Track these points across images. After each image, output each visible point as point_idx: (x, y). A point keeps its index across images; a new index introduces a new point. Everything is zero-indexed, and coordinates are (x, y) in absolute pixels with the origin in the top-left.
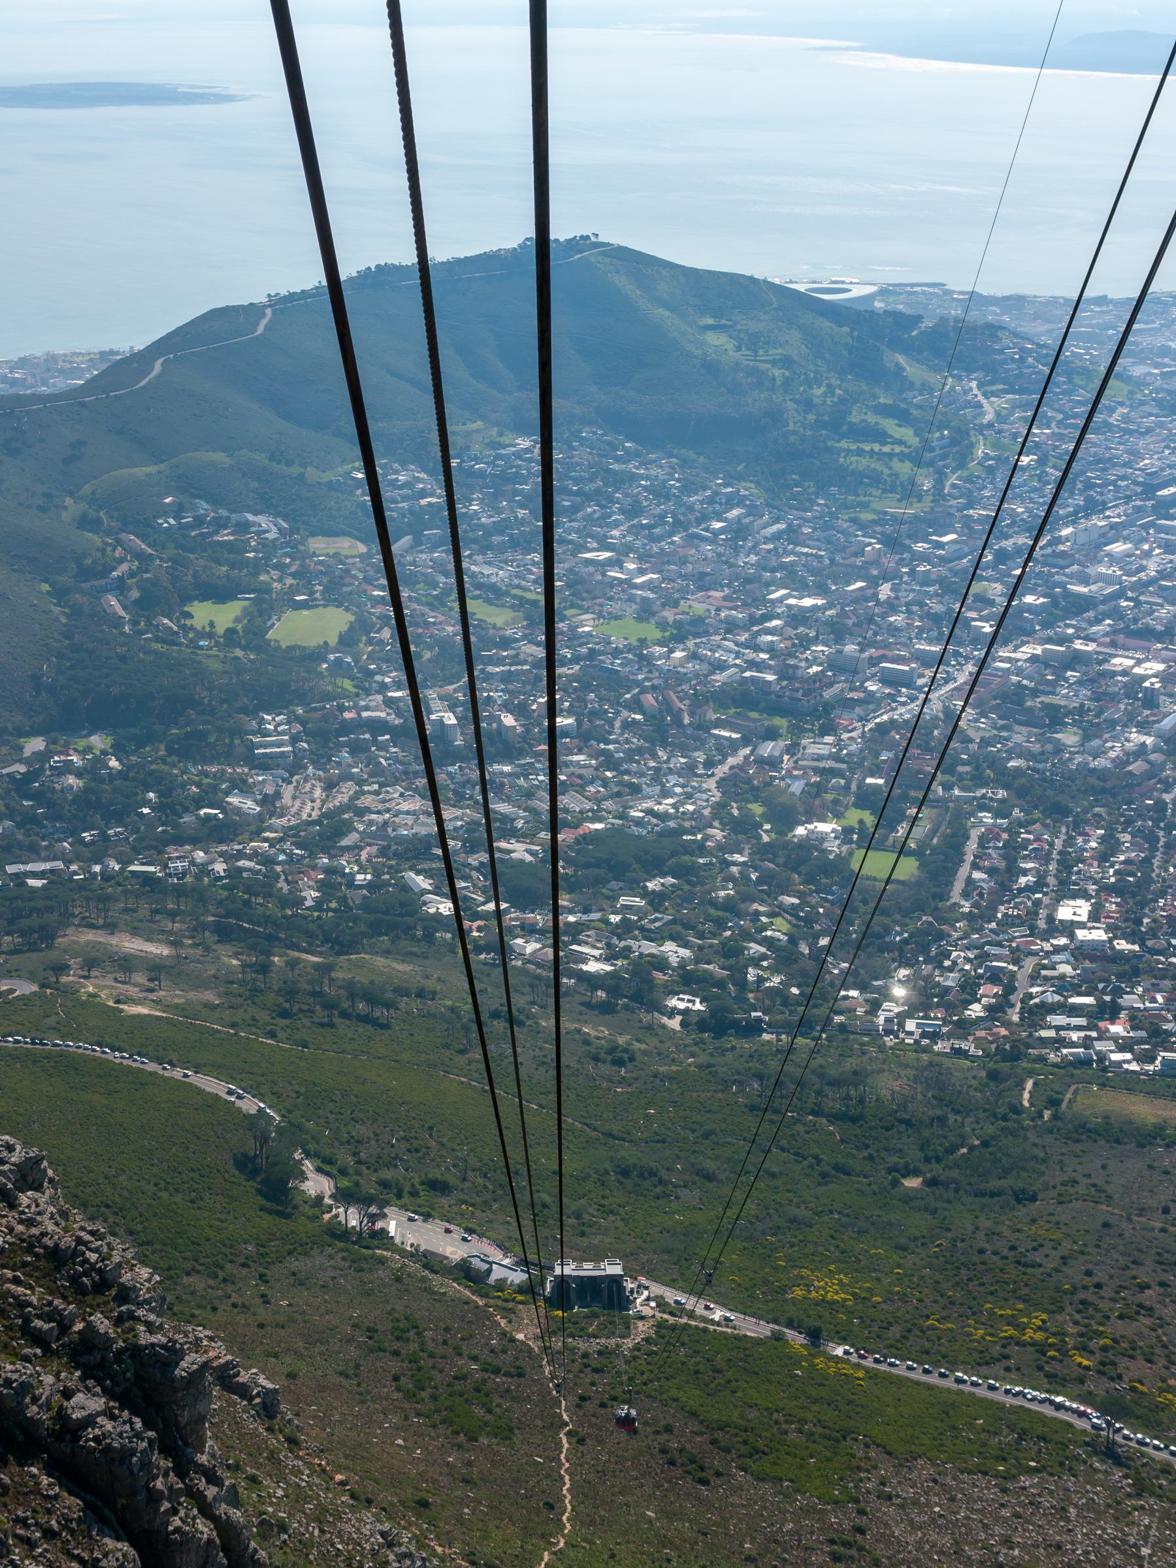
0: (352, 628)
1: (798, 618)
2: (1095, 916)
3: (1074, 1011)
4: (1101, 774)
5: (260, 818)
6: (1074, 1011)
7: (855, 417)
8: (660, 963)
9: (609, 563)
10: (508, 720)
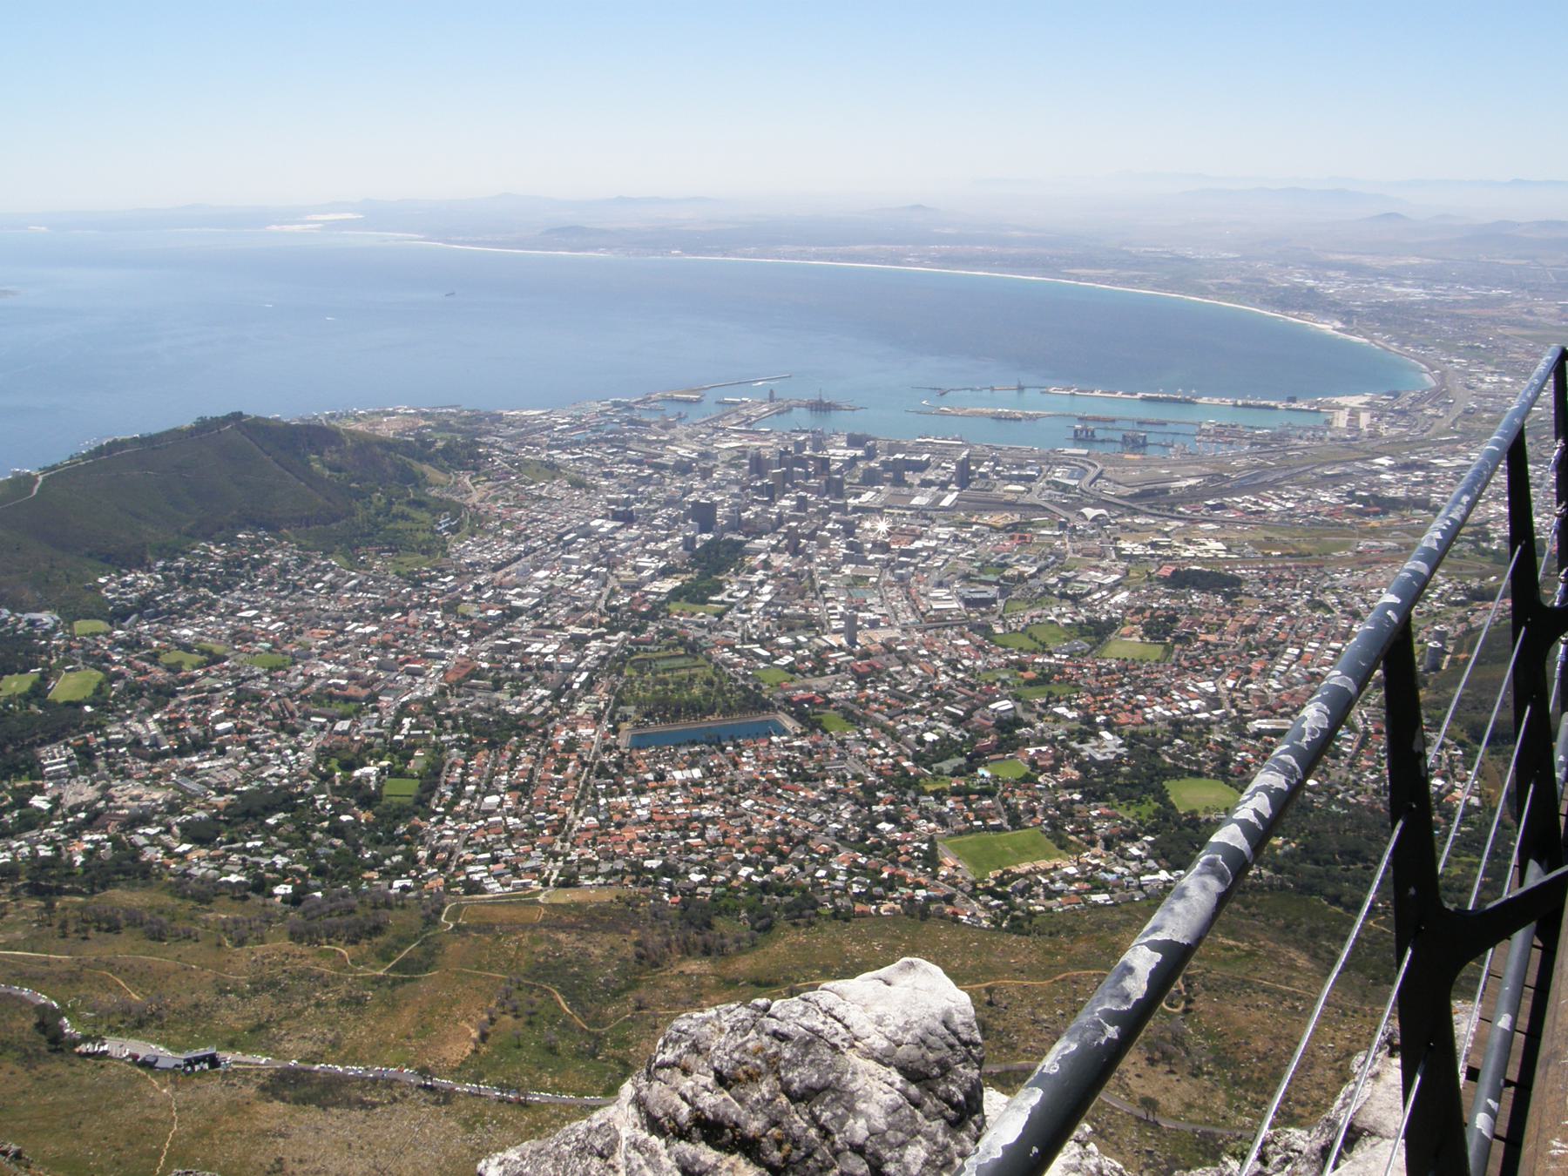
0: (101, 684)
1: (365, 638)
2: (500, 805)
3: (481, 862)
4: (519, 717)
5: (51, 811)
6: (481, 862)
7: (395, 509)
8: (272, 867)
9: (255, 617)
10: (194, 730)
